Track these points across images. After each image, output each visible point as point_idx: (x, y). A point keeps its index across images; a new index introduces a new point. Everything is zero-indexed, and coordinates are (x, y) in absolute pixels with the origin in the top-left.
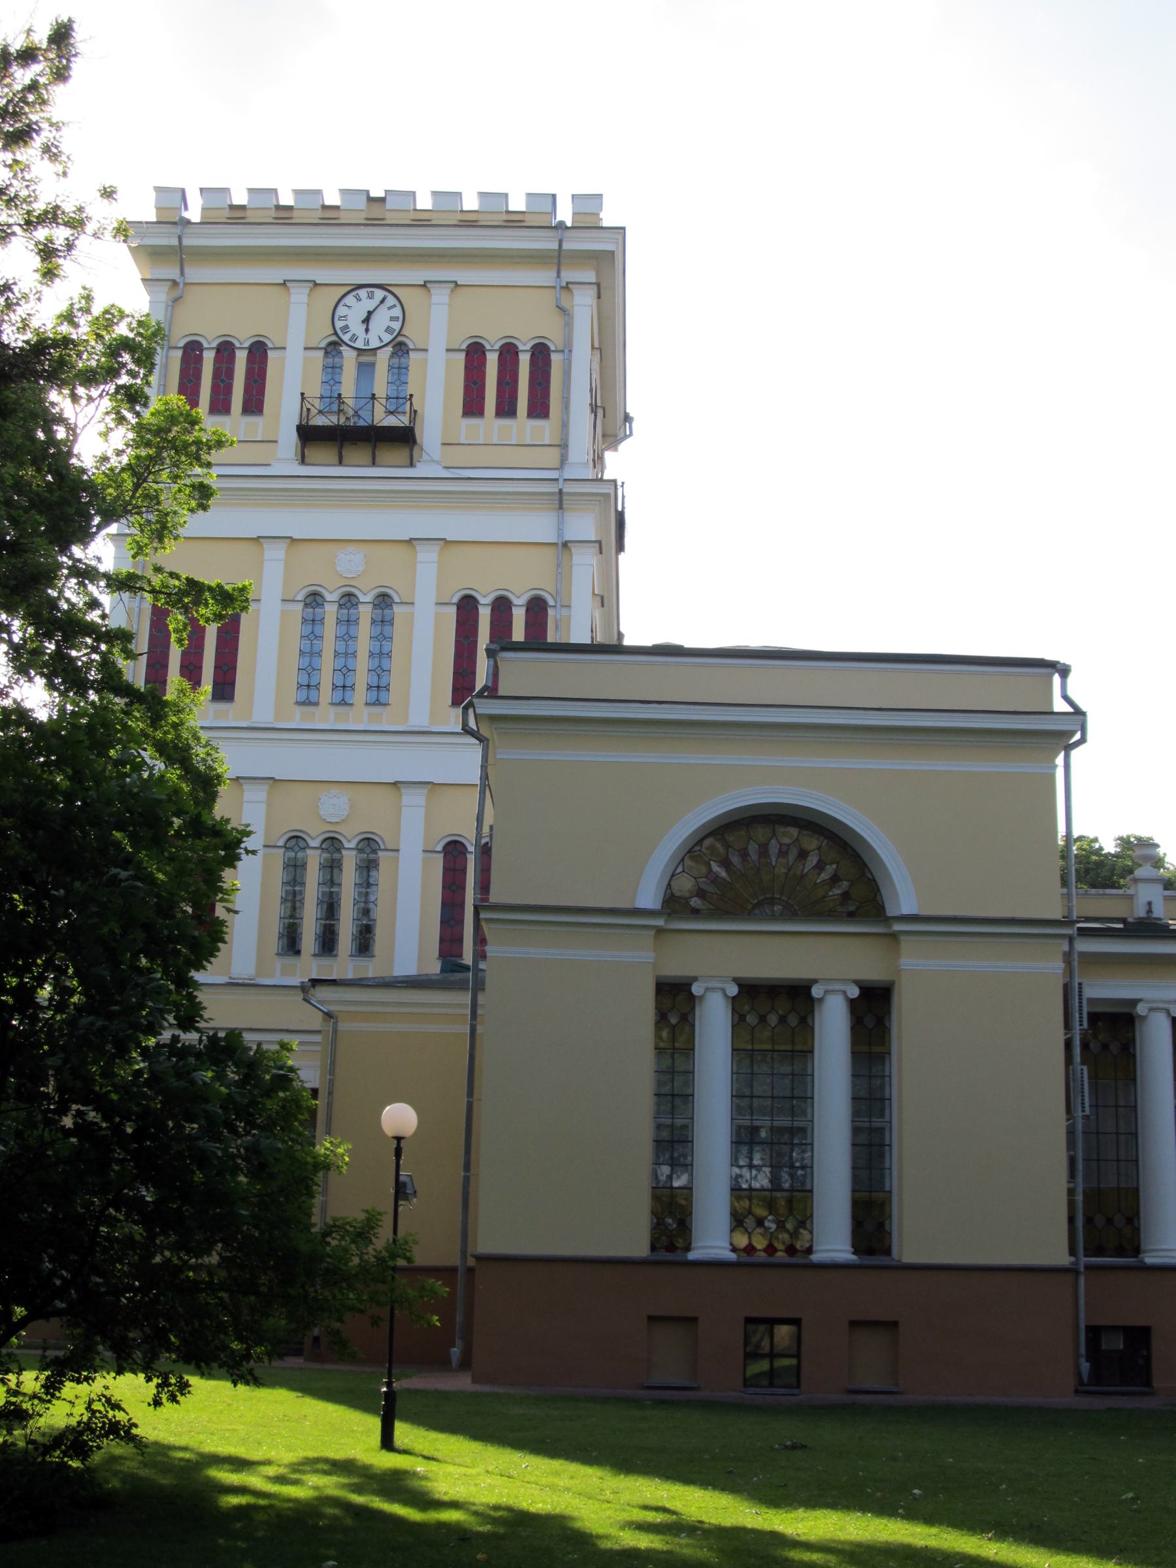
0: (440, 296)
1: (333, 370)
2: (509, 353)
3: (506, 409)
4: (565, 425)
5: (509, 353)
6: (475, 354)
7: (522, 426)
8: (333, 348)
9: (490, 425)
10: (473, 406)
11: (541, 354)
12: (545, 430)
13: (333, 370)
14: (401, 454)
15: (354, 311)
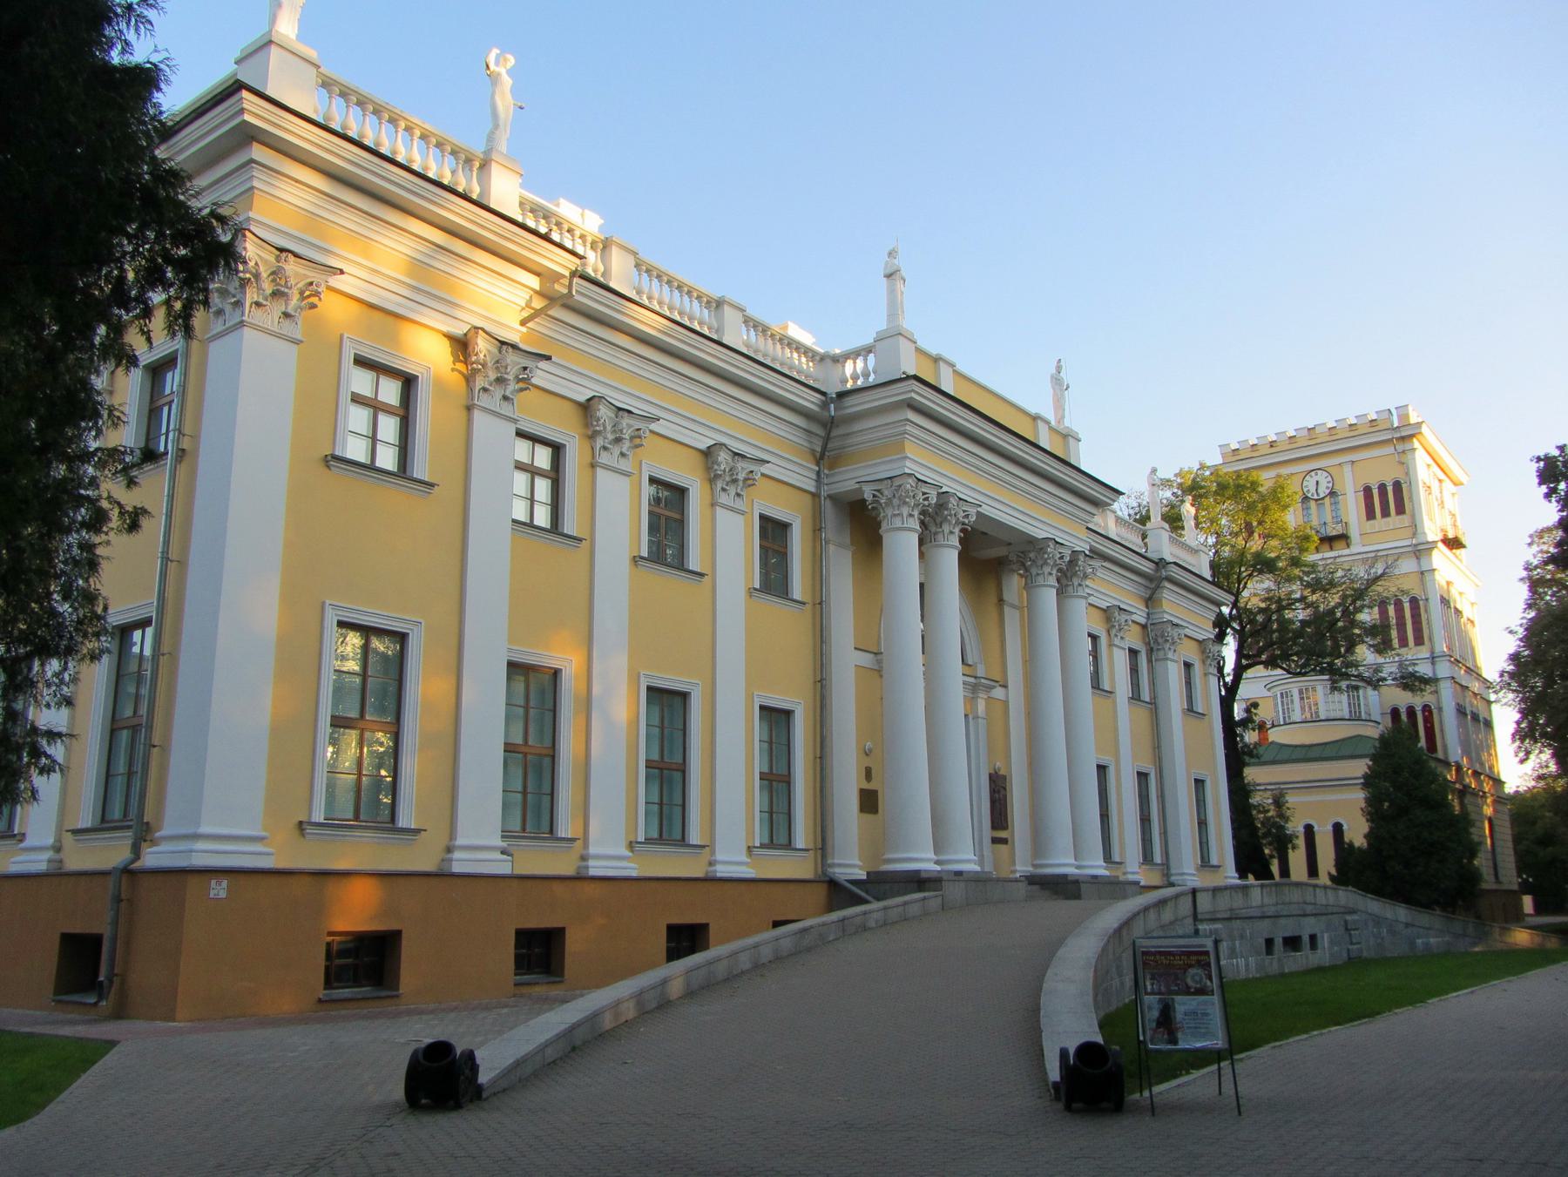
0: (1347, 469)
1: (1306, 509)
2: (1382, 488)
3: (1386, 513)
4: (1413, 516)
5: (1382, 488)
6: (1367, 491)
7: (1394, 520)
8: (1306, 499)
9: (1379, 523)
10: (1370, 515)
11: (1397, 486)
12: (1404, 520)
13: (1306, 509)
14: (1343, 543)
15: (1310, 484)
